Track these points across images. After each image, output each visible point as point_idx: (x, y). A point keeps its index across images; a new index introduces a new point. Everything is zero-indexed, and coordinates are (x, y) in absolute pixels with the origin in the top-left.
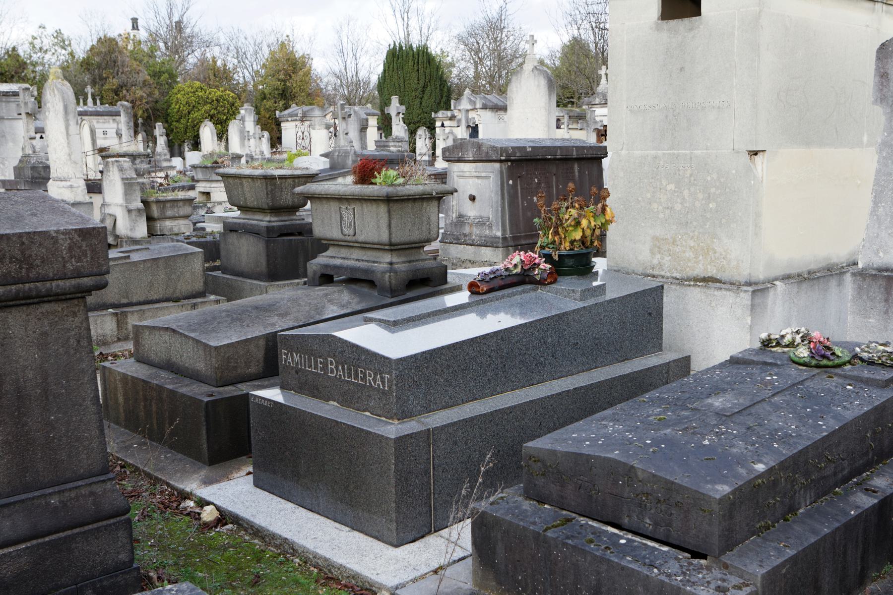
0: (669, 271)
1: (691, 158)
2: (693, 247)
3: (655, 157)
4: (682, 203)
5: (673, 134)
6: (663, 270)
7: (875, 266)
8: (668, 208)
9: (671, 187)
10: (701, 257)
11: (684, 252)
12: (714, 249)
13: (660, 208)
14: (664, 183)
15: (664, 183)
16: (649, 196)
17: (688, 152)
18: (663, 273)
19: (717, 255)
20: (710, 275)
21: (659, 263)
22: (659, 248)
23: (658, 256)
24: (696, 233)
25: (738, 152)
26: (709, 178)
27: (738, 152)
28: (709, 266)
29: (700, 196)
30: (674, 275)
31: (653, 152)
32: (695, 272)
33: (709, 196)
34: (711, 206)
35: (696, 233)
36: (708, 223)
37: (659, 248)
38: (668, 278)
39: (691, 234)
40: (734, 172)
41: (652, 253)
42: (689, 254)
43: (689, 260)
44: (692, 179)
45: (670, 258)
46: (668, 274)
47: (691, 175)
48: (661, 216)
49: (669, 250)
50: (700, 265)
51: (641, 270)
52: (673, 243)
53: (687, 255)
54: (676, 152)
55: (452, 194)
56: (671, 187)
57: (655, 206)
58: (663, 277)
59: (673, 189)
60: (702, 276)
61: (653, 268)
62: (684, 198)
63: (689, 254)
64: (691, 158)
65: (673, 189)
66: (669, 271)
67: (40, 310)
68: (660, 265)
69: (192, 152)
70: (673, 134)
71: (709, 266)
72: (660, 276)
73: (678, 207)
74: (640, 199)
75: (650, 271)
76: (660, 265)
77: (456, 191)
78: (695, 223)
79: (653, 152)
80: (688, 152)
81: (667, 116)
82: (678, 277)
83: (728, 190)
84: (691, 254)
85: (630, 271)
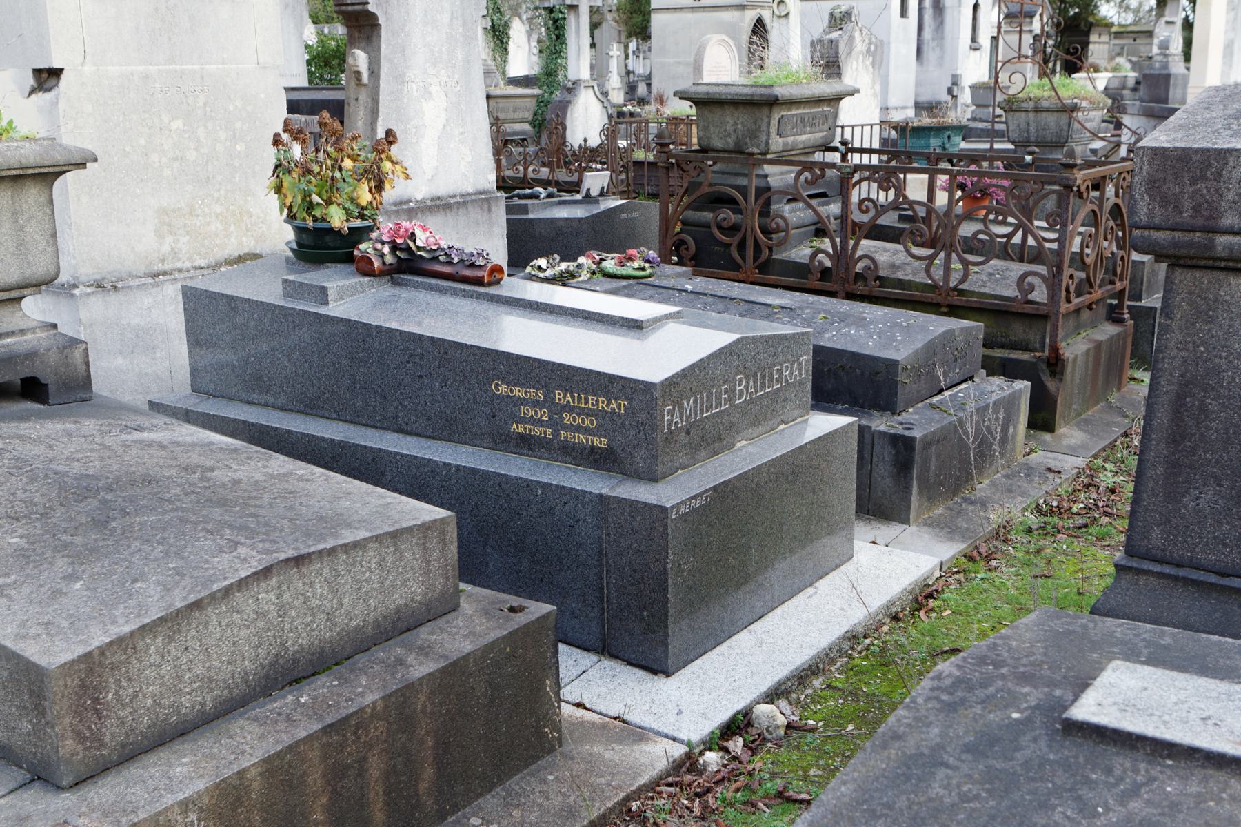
0: (189, 259)
1: (202, 78)
2: (221, 214)
3: (146, 77)
4: (196, 149)
5: (170, 39)
6: (179, 260)
7: (391, 201)
8: (176, 159)
9: (178, 124)
10: (232, 228)
11: (208, 224)
12: (248, 212)
13: (164, 160)
14: (166, 119)
15: (166, 119)
16: (142, 142)
17: (197, 67)
18: (179, 265)
19: (253, 219)
20: (246, 250)
21: (172, 249)
22: (169, 225)
23: (170, 239)
24: (222, 192)
25: (265, 68)
26: (231, 107)
27: (265, 68)
28: (244, 239)
29: (222, 135)
30: (196, 264)
31: (141, 68)
32: (227, 251)
33: (235, 134)
34: (238, 148)
35: (222, 192)
36: (238, 175)
37: (169, 225)
38: (188, 271)
39: (216, 195)
40: (262, 96)
41: (160, 236)
42: (216, 226)
43: (216, 235)
44: (208, 109)
45: (188, 237)
46: (188, 265)
47: (205, 104)
48: (167, 172)
49: (185, 226)
50: (233, 240)
51: (142, 269)
52: (191, 214)
53: (213, 228)
54: (178, 67)
55: (83, 165)
56: (178, 124)
57: (155, 157)
58: (180, 271)
59: (181, 127)
60: (236, 254)
61: (163, 261)
62: (199, 141)
63: (216, 226)
64: (202, 78)
65: (181, 127)
66: (189, 259)
67: (269, 707)
68: (175, 253)
69: (61, 81)
70: (170, 39)
71: (244, 239)
72: (175, 270)
73: (191, 155)
74: (127, 149)
75: (159, 267)
76: (175, 253)
77: (96, 160)
78: (219, 178)
79: (141, 68)
80: (197, 67)
81: (156, 9)
82: (203, 265)
83: (257, 123)
84: (219, 225)
85: (124, 275)
